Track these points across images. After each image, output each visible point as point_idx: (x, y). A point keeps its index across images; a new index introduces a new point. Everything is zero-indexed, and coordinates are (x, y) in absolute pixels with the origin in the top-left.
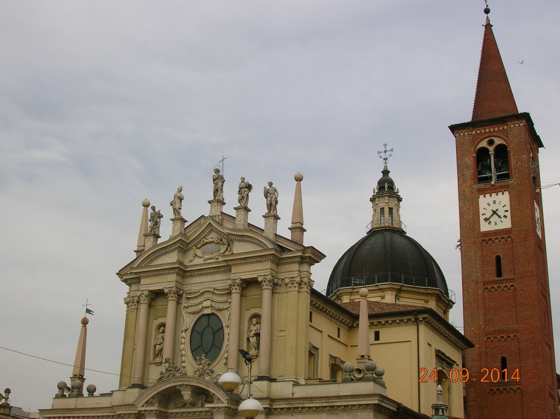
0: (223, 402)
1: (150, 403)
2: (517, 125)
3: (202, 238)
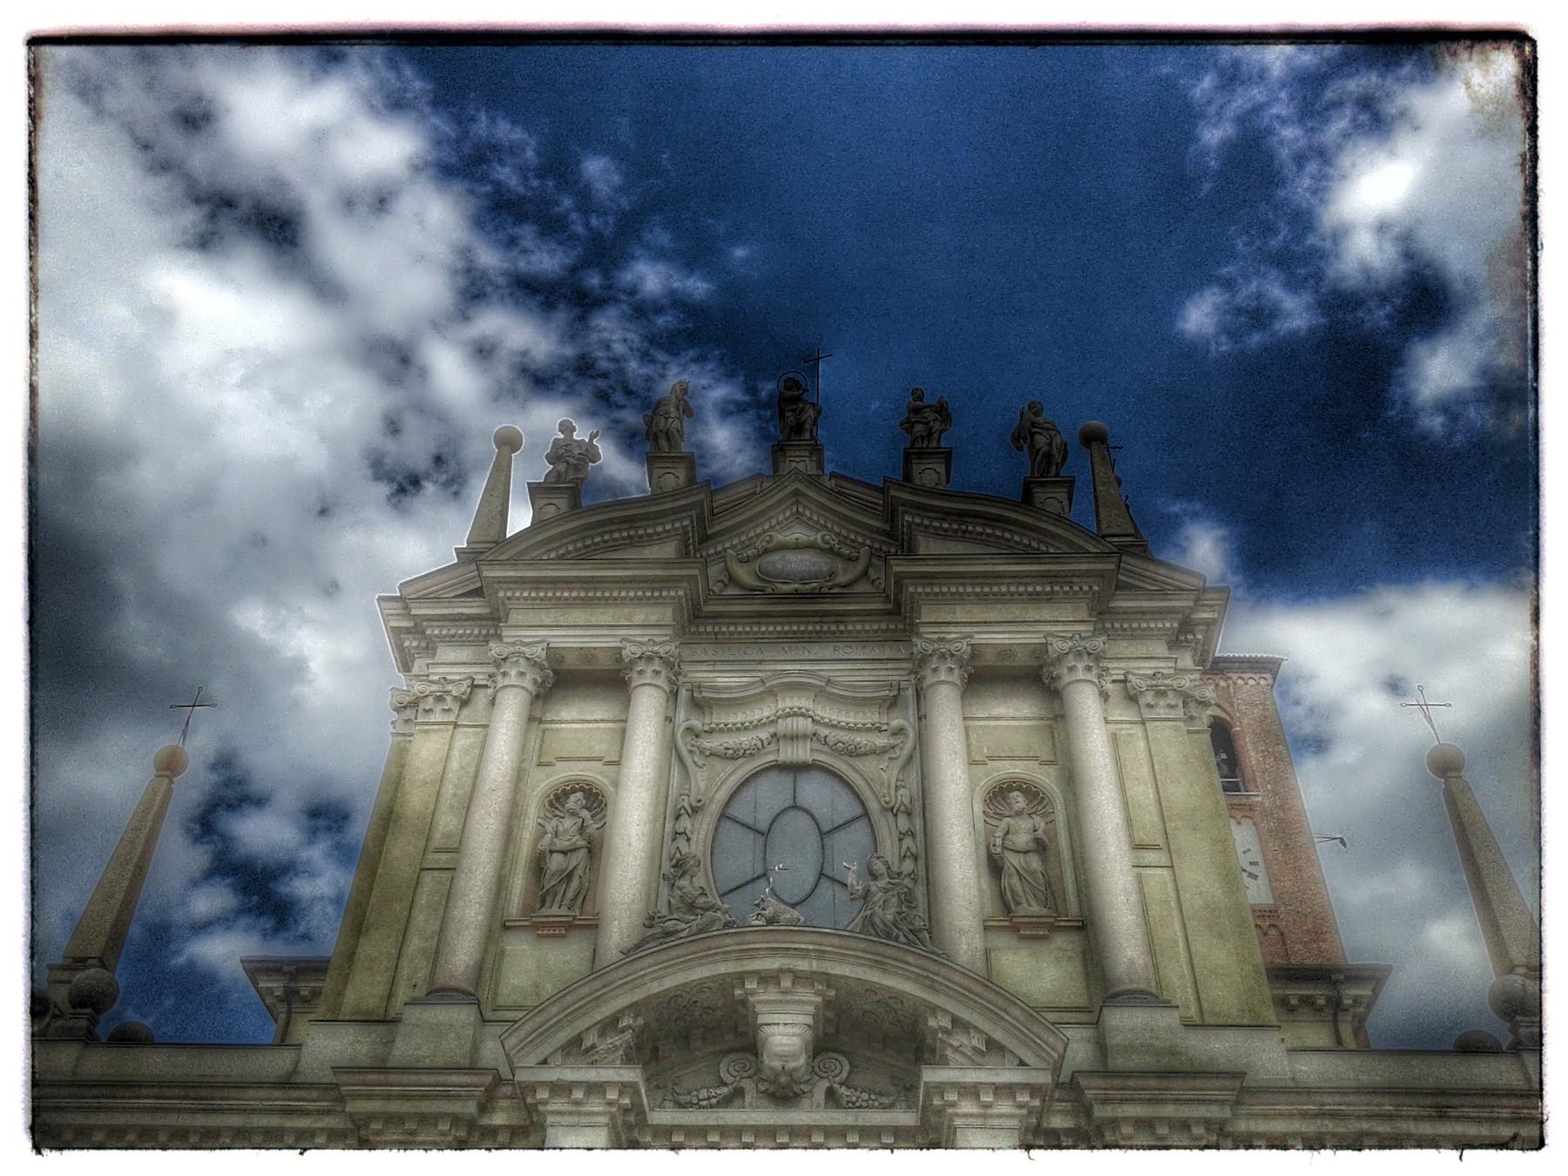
0: (1022, 1063)
1: (587, 1050)
2: (1252, 682)
3: (768, 531)
